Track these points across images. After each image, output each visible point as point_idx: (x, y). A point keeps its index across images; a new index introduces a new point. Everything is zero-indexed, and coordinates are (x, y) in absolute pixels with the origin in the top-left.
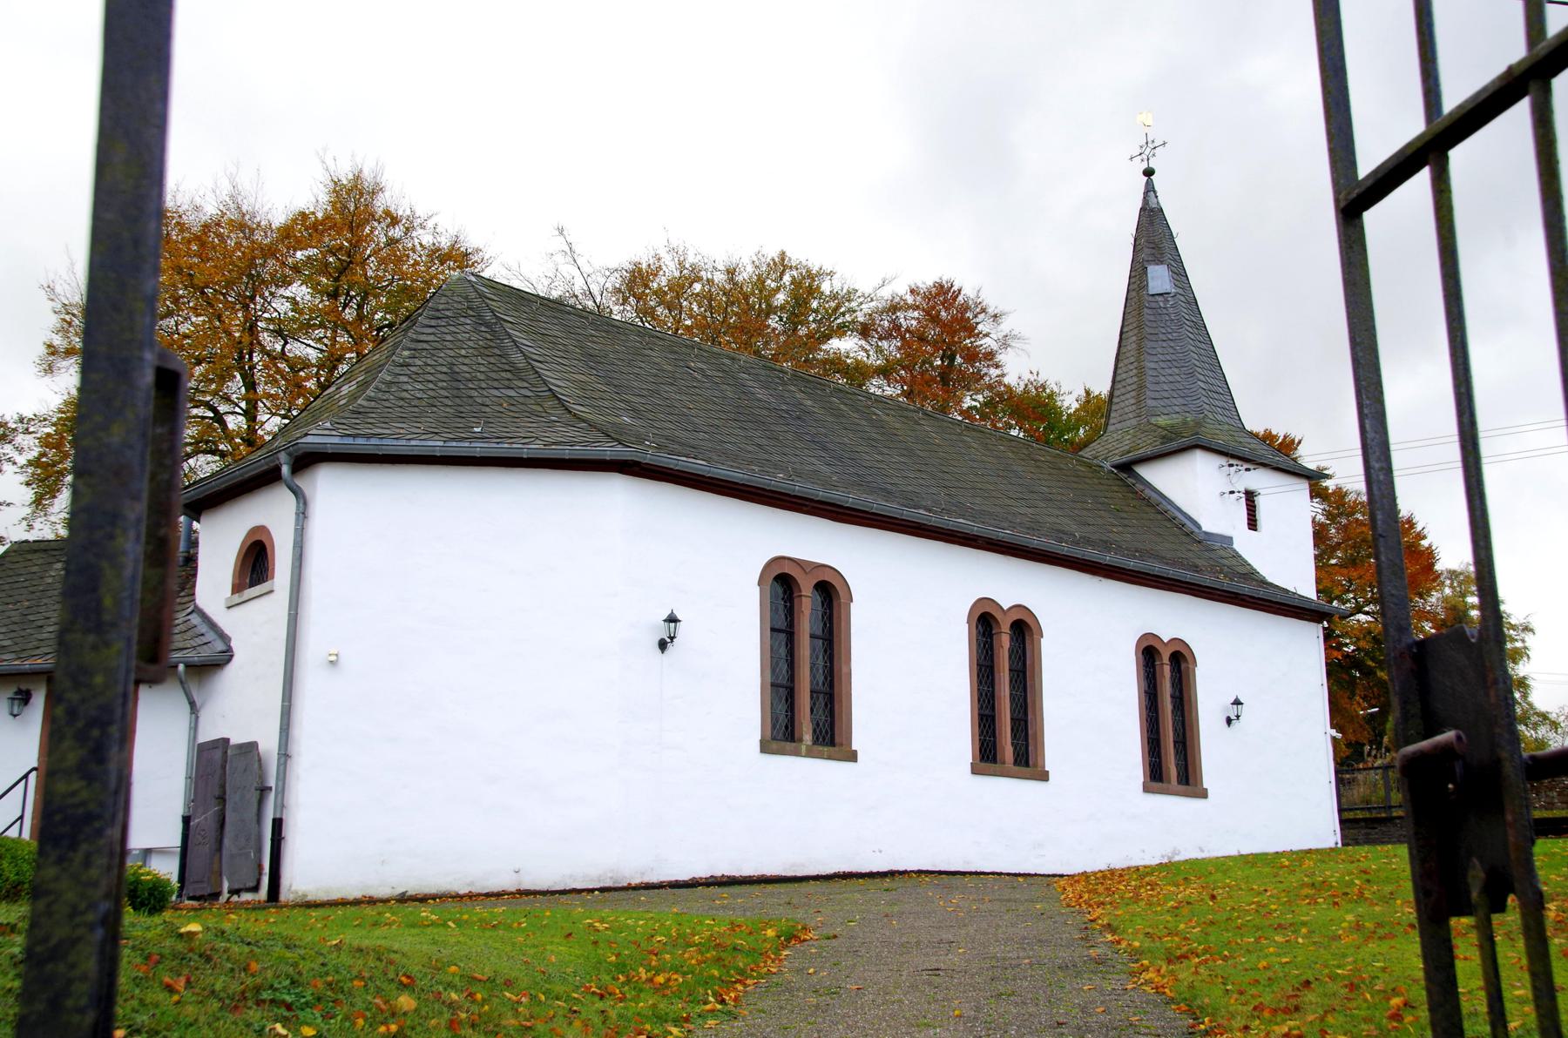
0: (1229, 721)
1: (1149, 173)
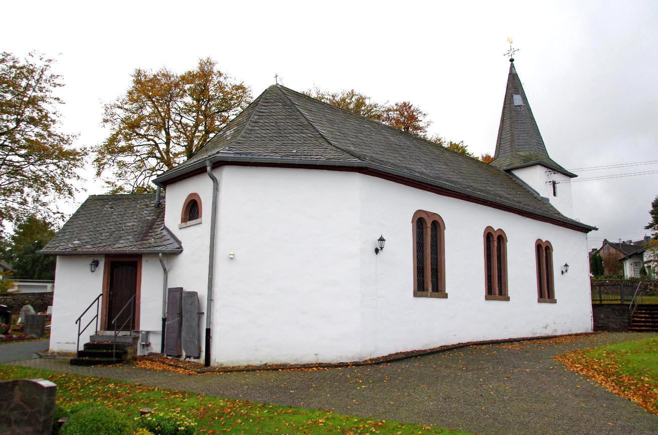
0: (562, 272)
1: (512, 60)
